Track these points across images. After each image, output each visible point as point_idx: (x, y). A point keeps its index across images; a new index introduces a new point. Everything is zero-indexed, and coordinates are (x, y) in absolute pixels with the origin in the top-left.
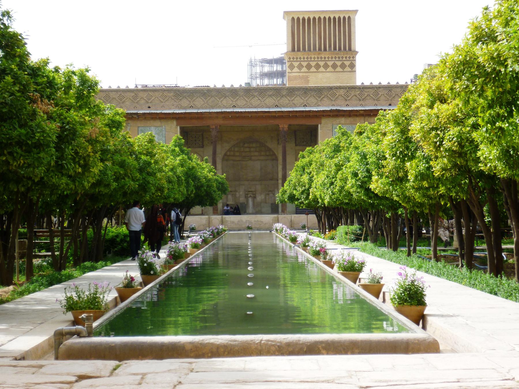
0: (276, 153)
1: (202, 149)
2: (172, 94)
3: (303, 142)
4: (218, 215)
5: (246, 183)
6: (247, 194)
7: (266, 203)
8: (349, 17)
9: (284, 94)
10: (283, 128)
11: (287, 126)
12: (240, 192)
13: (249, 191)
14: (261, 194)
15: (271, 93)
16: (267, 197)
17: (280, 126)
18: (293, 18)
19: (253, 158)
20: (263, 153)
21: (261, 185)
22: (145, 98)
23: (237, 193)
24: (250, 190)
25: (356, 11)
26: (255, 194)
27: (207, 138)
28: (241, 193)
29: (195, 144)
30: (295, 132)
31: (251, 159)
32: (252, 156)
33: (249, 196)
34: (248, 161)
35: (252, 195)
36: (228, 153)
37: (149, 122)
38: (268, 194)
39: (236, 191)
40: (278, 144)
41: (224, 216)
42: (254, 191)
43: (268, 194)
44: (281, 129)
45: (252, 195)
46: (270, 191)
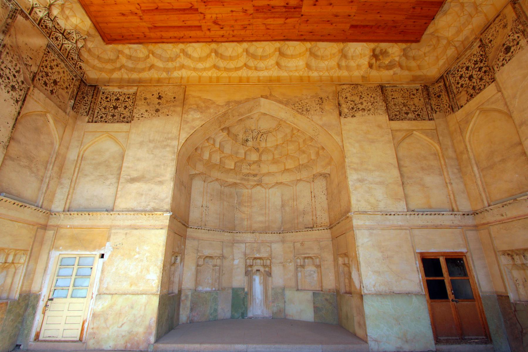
1: (124, 126)
3: (407, 113)
5: (249, 237)
7: (298, 290)
12: (233, 259)
13: (255, 258)
16: (299, 274)
19: (266, 180)
20: (290, 164)
21: (283, 241)
24: (258, 256)
27: (145, 99)
29: (113, 116)
30: (382, 88)
31: (259, 183)
32: (264, 175)
33: (255, 268)
34: (254, 186)
35: (262, 269)
38: (303, 266)
40: (340, 115)
42: (268, 259)
45: (262, 269)
46: (308, 258)
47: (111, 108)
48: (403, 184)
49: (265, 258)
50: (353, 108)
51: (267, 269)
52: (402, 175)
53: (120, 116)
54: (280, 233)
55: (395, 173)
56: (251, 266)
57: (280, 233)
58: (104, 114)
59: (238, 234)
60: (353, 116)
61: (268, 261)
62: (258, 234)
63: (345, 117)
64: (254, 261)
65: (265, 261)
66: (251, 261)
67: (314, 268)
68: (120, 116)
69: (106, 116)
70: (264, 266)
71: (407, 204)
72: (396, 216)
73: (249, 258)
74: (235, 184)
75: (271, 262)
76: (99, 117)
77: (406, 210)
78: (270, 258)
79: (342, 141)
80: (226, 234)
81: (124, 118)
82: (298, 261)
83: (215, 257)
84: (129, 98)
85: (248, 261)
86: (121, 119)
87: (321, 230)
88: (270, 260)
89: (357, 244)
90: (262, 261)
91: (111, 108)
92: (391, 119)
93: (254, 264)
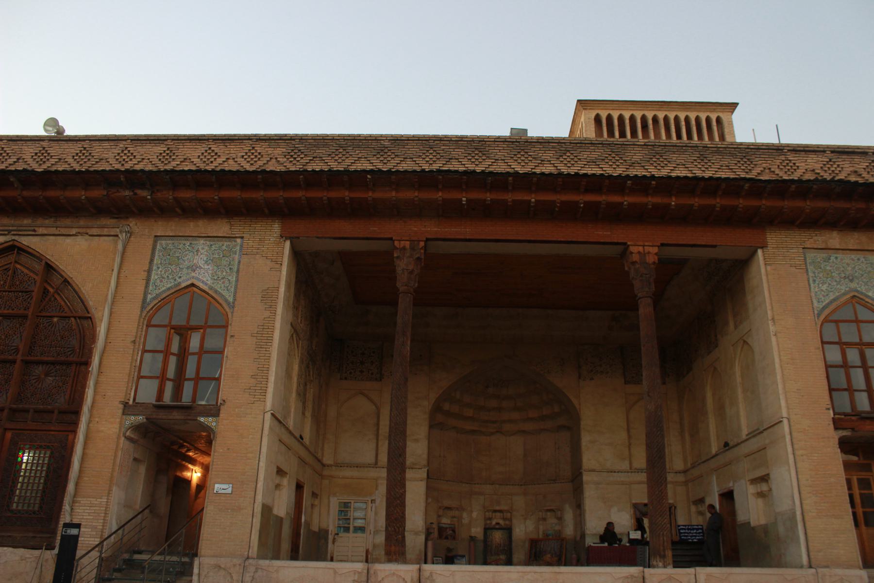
0: (575, 402)
2: (279, 151)
4: (405, 562)
6: (490, 519)
8: (719, 121)
9: (636, 158)
10: (642, 255)
11: (656, 250)
12: (472, 511)
13: (495, 511)
14: (525, 519)
15: (594, 155)
17: (633, 249)
18: (598, 119)
22: (196, 160)
23: (465, 515)
24: (497, 508)
25: (734, 106)
26: (510, 520)
28: (475, 514)
29: (362, 372)
36: (446, 406)
37: (192, 224)
38: (544, 519)
39: (461, 509)
40: (580, 377)
41: (428, 568)
42: (508, 511)
43: (544, 519)
44: (635, 258)
47: (358, 363)
48: (630, 444)
49: (506, 510)
50: (592, 371)
51: (507, 522)
52: (629, 437)
53: (368, 371)
54: (521, 485)
55: (624, 435)
56: (490, 519)
57: (521, 485)
58: (352, 369)
59: (477, 485)
60: (592, 379)
61: (509, 514)
62: (497, 486)
63: (584, 380)
64: (494, 514)
65: (505, 514)
66: (491, 513)
67: (555, 521)
68: (368, 371)
69: (355, 372)
70: (504, 519)
71: (631, 464)
72: (620, 474)
73: (488, 511)
74: (473, 432)
75: (511, 515)
76: (348, 372)
77: (628, 468)
78: (511, 511)
79: (580, 405)
80: (464, 485)
81: (372, 374)
82: (541, 513)
83: (454, 508)
84: (374, 352)
85: (487, 513)
86: (370, 375)
87: (563, 483)
88: (510, 513)
89: (585, 496)
90: (502, 514)
91: (358, 363)
92: (626, 382)
93: (494, 517)
